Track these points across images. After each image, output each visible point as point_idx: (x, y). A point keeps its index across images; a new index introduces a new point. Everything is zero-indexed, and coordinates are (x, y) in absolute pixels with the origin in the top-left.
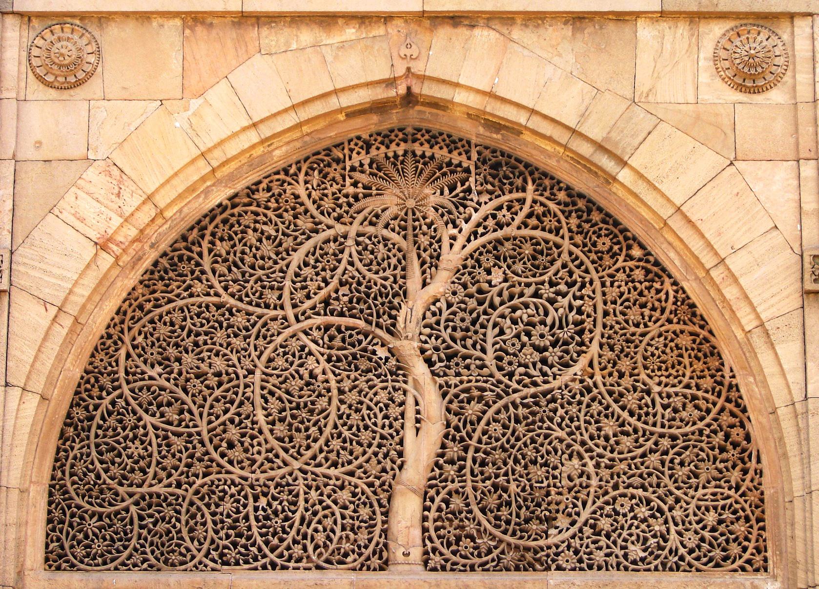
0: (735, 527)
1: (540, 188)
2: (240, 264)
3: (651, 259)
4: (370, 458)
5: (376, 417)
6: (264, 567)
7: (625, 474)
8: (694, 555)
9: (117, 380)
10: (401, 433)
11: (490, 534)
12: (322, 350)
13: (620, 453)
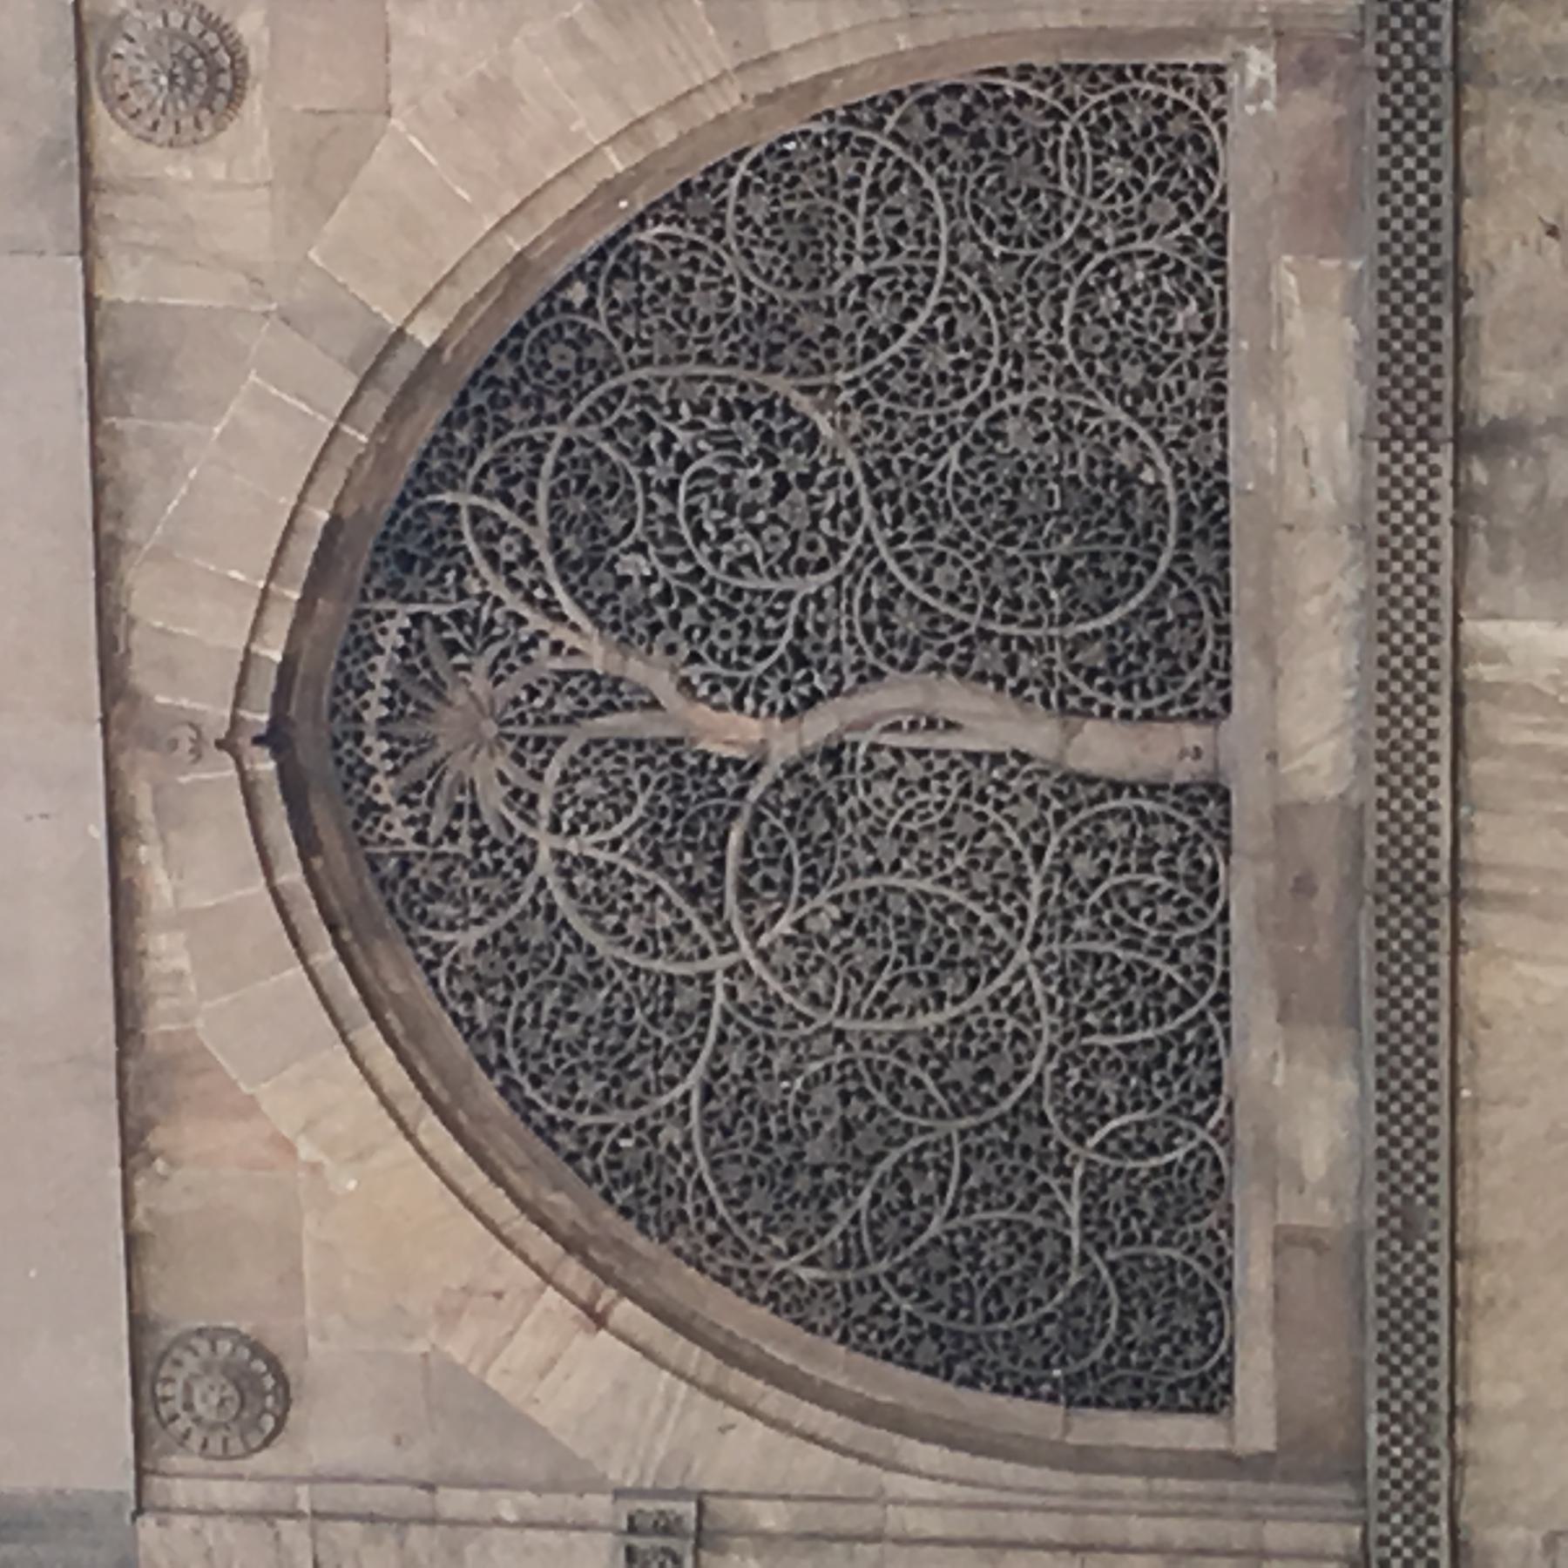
2: (621, 1055)
4: (1008, 817)
6: (1224, 1017)
7: (1031, 332)
11: (1155, 593)
13: (989, 339)
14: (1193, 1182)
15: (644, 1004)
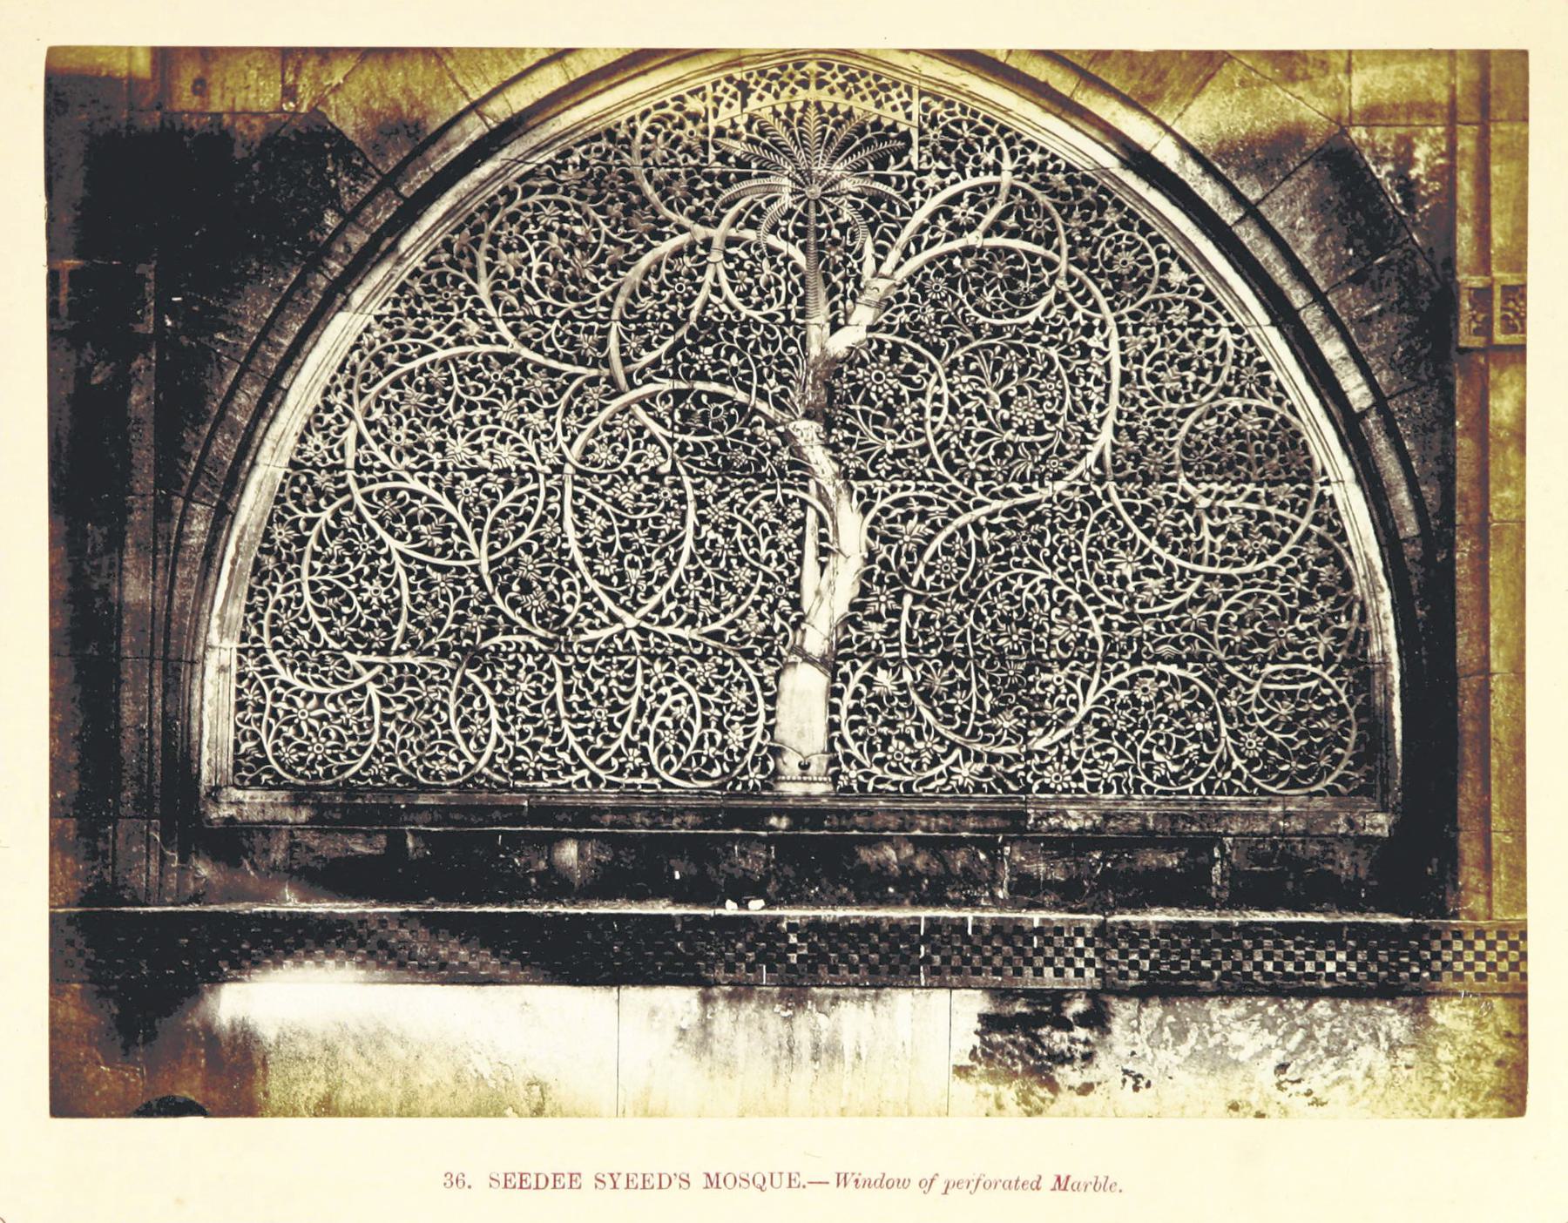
3: (1200, 287)
4: (747, 611)
5: (757, 544)
7: (1150, 638)
9: (343, 479)
10: (797, 571)
11: (937, 734)
12: (669, 434)
13: (1144, 605)
15: (580, 309)
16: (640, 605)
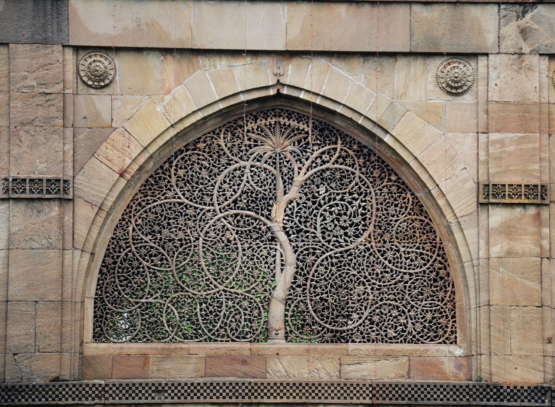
0: (441, 321)
1: (344, 143)
3: (401, 181)
4: (258, 284)
6: (205, 340)
7: (386, 293)
8: (420, 335)
9: (128, 243)
10: (274, 271)
11: (319, 324)
13: (384, 282)
14: (159, 332)
15: (205, 188)
16: (224, 283)
